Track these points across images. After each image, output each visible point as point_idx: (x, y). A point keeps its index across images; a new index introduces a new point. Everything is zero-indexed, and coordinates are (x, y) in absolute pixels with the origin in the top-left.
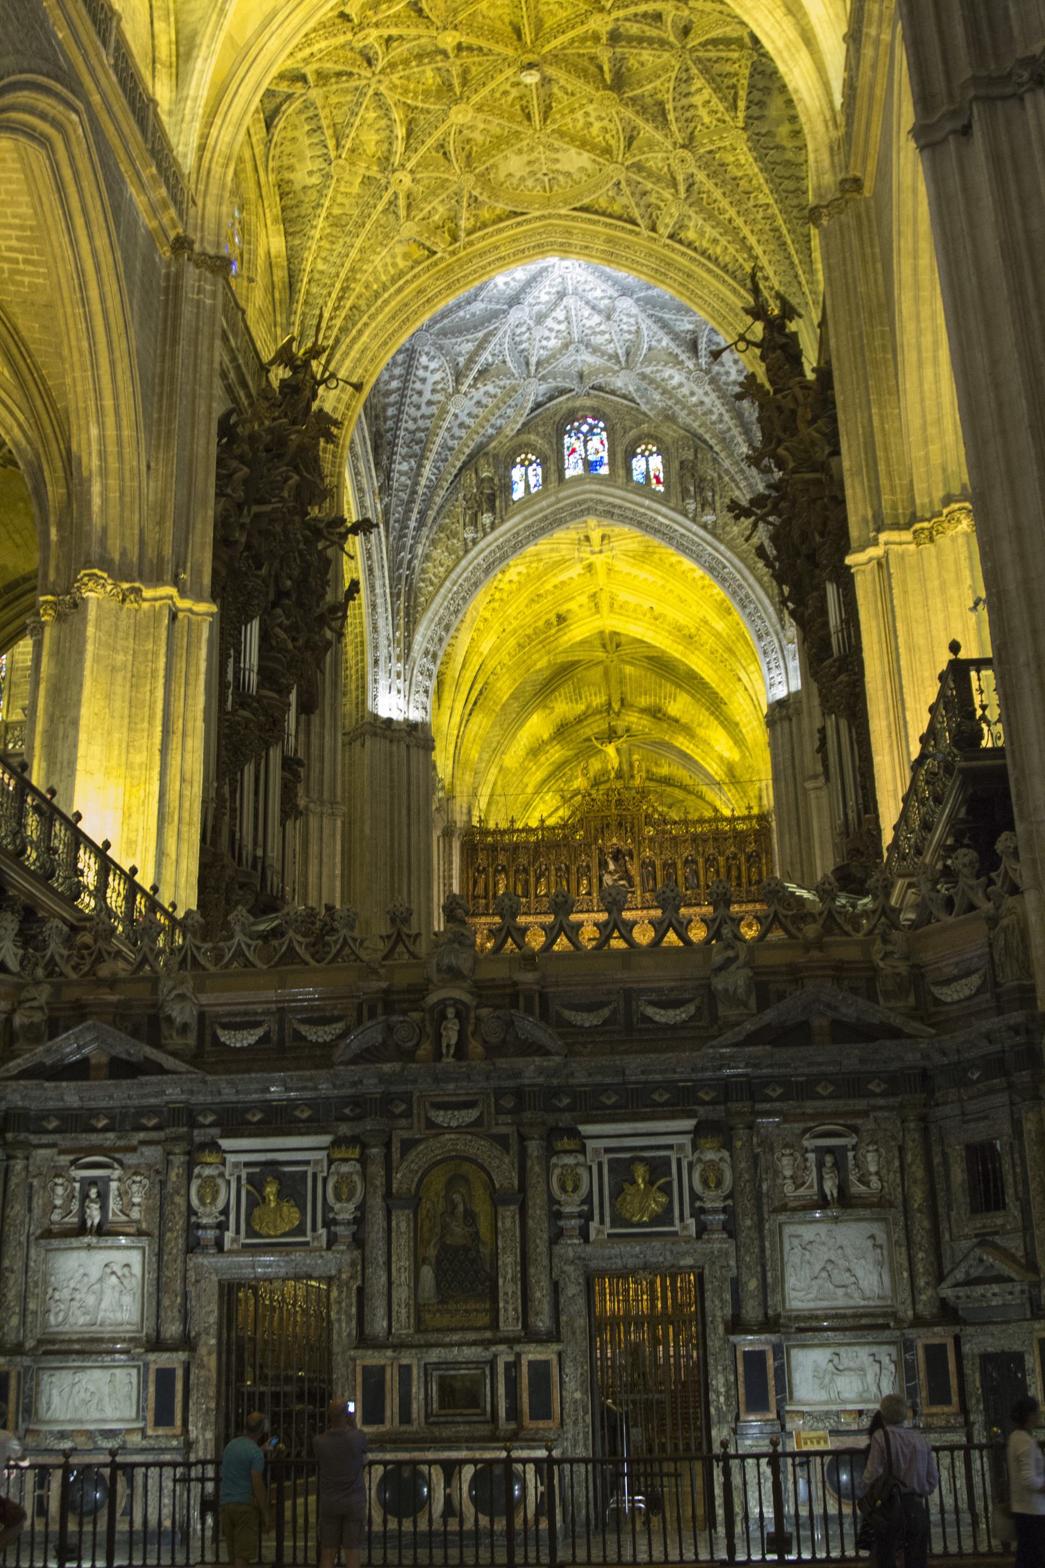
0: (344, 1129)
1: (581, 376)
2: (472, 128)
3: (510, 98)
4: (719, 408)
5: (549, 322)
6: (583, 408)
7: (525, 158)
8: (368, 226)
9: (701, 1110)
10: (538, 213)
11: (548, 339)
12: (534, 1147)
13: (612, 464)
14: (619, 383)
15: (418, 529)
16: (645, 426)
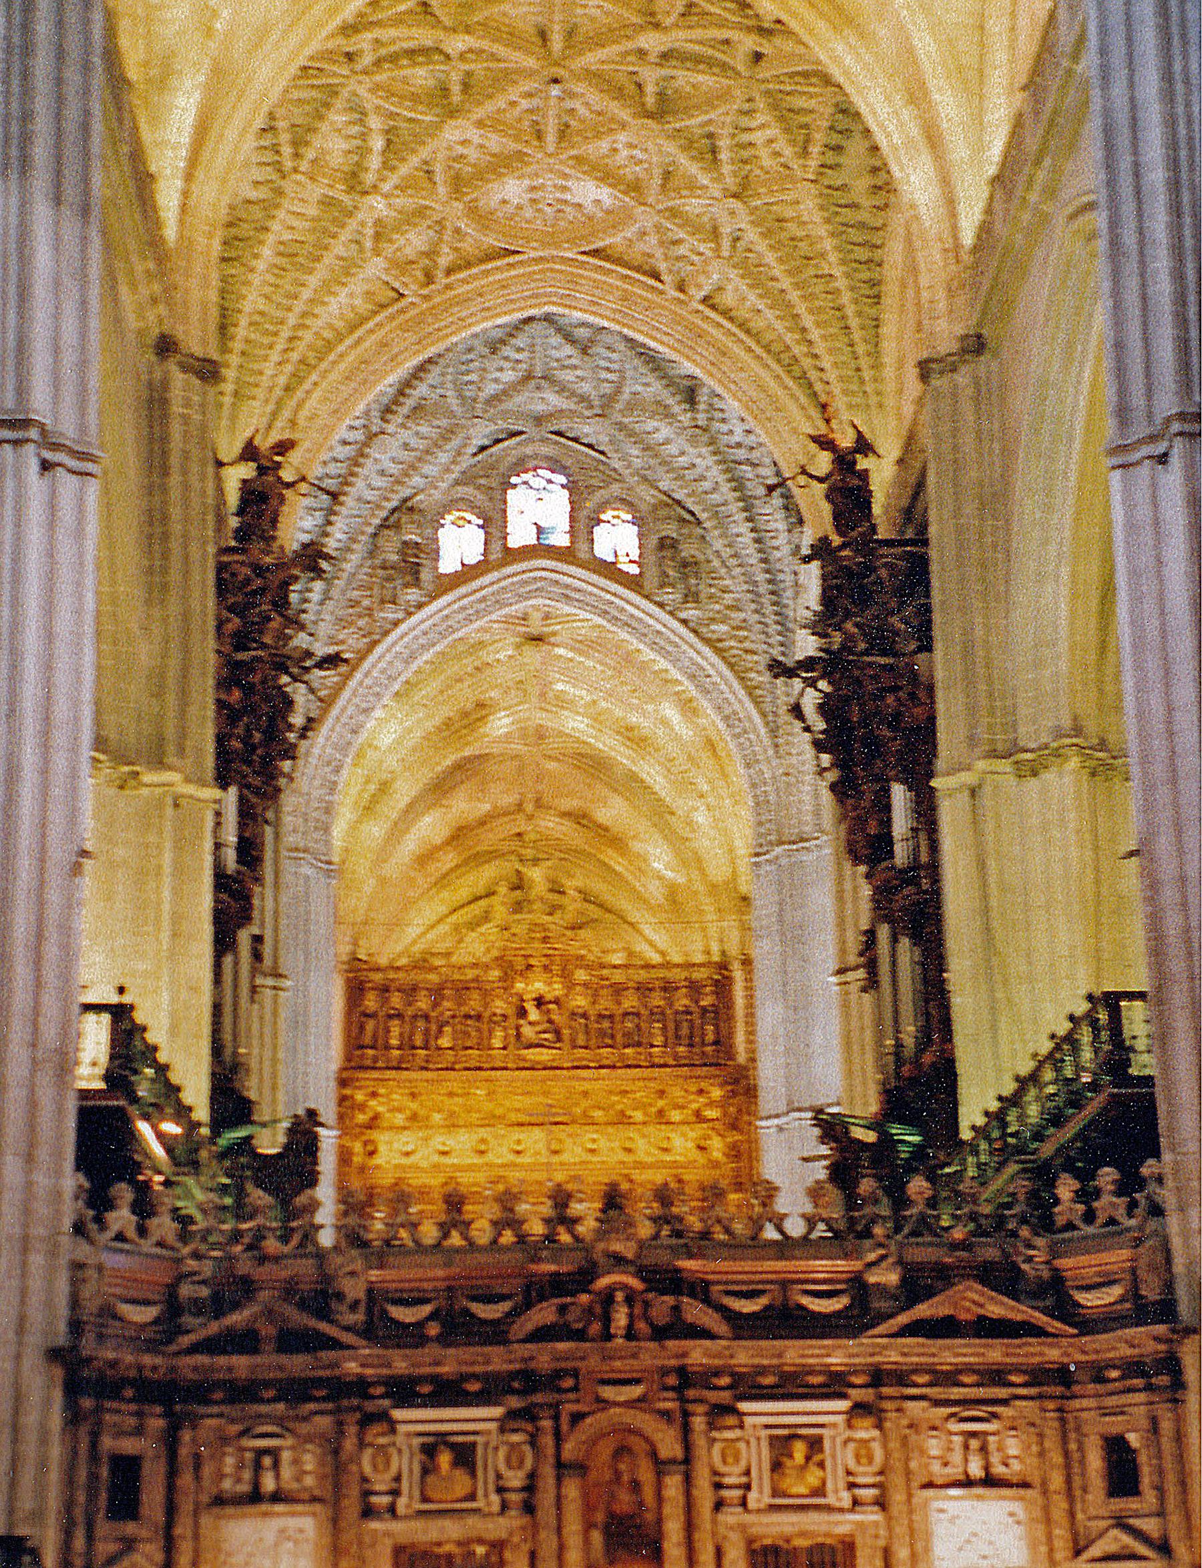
0: (515, 1402)
1: (539, 420)
2: (464, 142)
3: (516, 112)
4: (715, 474)
5: (507, 351)
6: (536, 456)
7: (527, 182)
8: (326, 261)
9: (852, 1392)
10: (533, 254)
11: (501, 369)
12: (698, 1423)
13: (572, 532)
14: (586, 429)
15: (322, 603)
16: (615, 488)
